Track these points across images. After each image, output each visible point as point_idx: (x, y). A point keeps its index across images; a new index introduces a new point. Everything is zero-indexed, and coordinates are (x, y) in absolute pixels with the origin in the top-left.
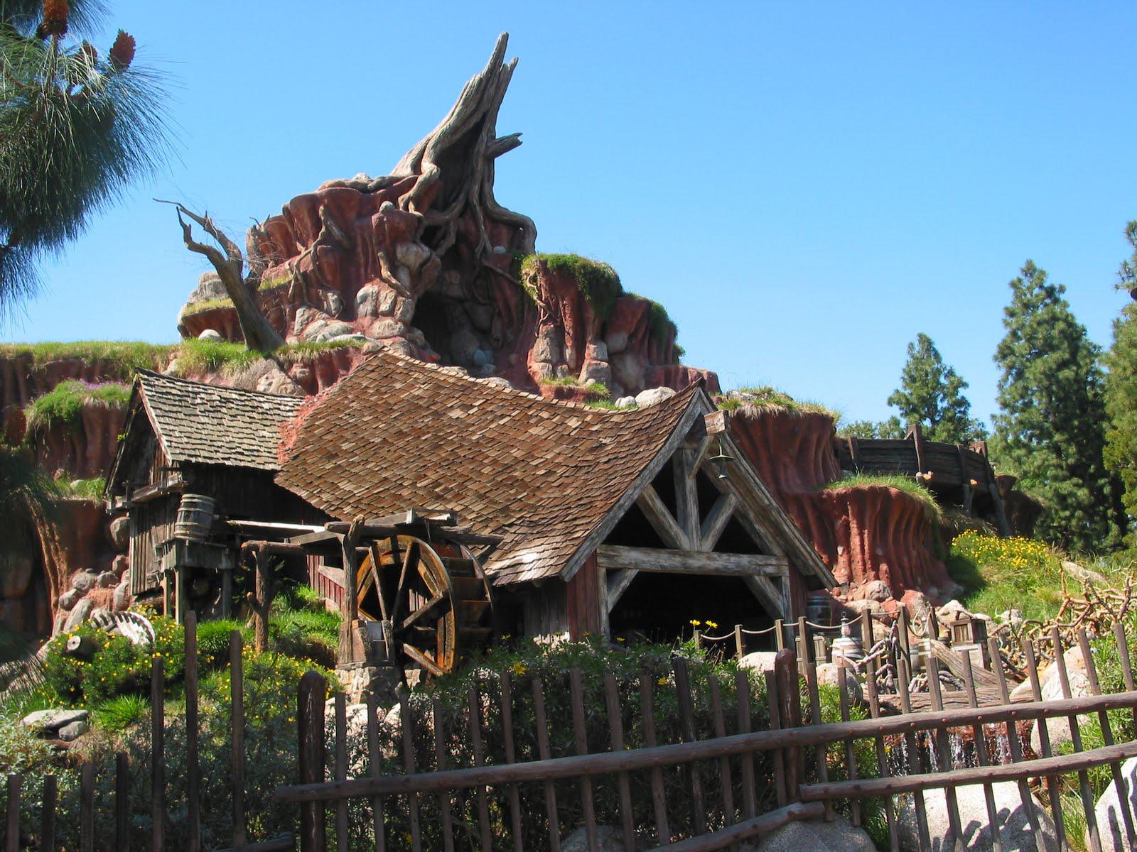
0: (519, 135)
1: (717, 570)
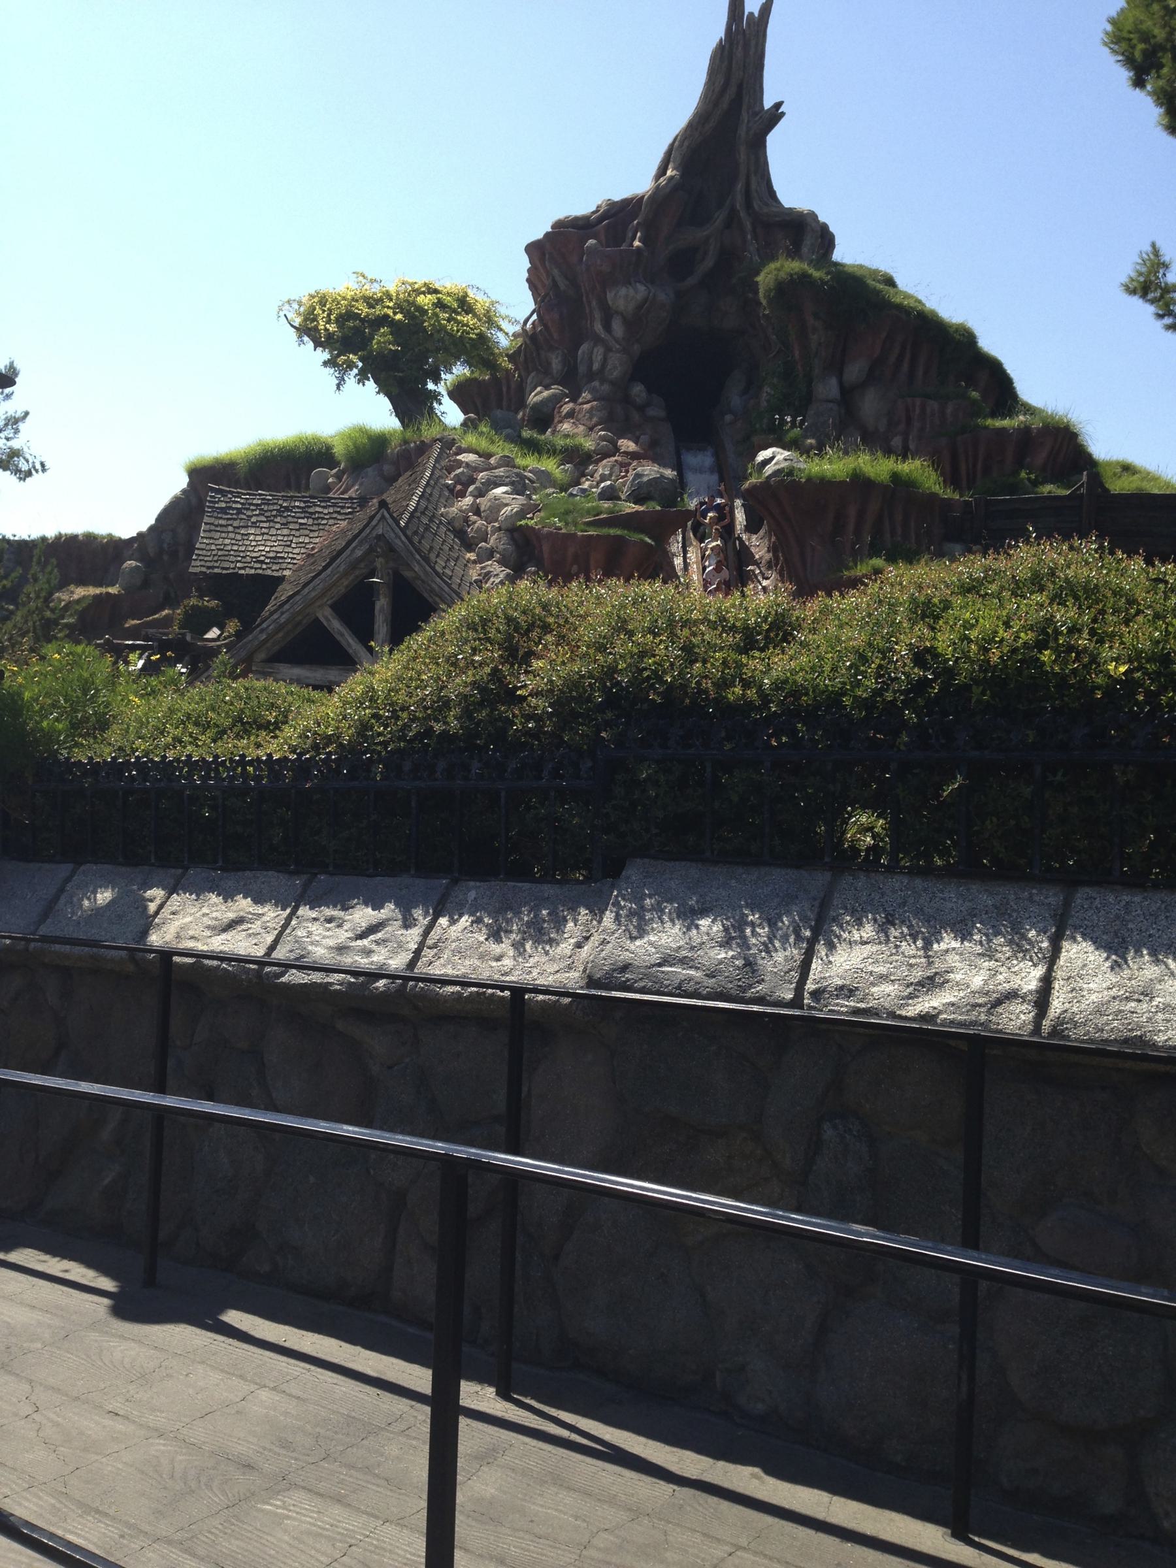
0: (778, 105)
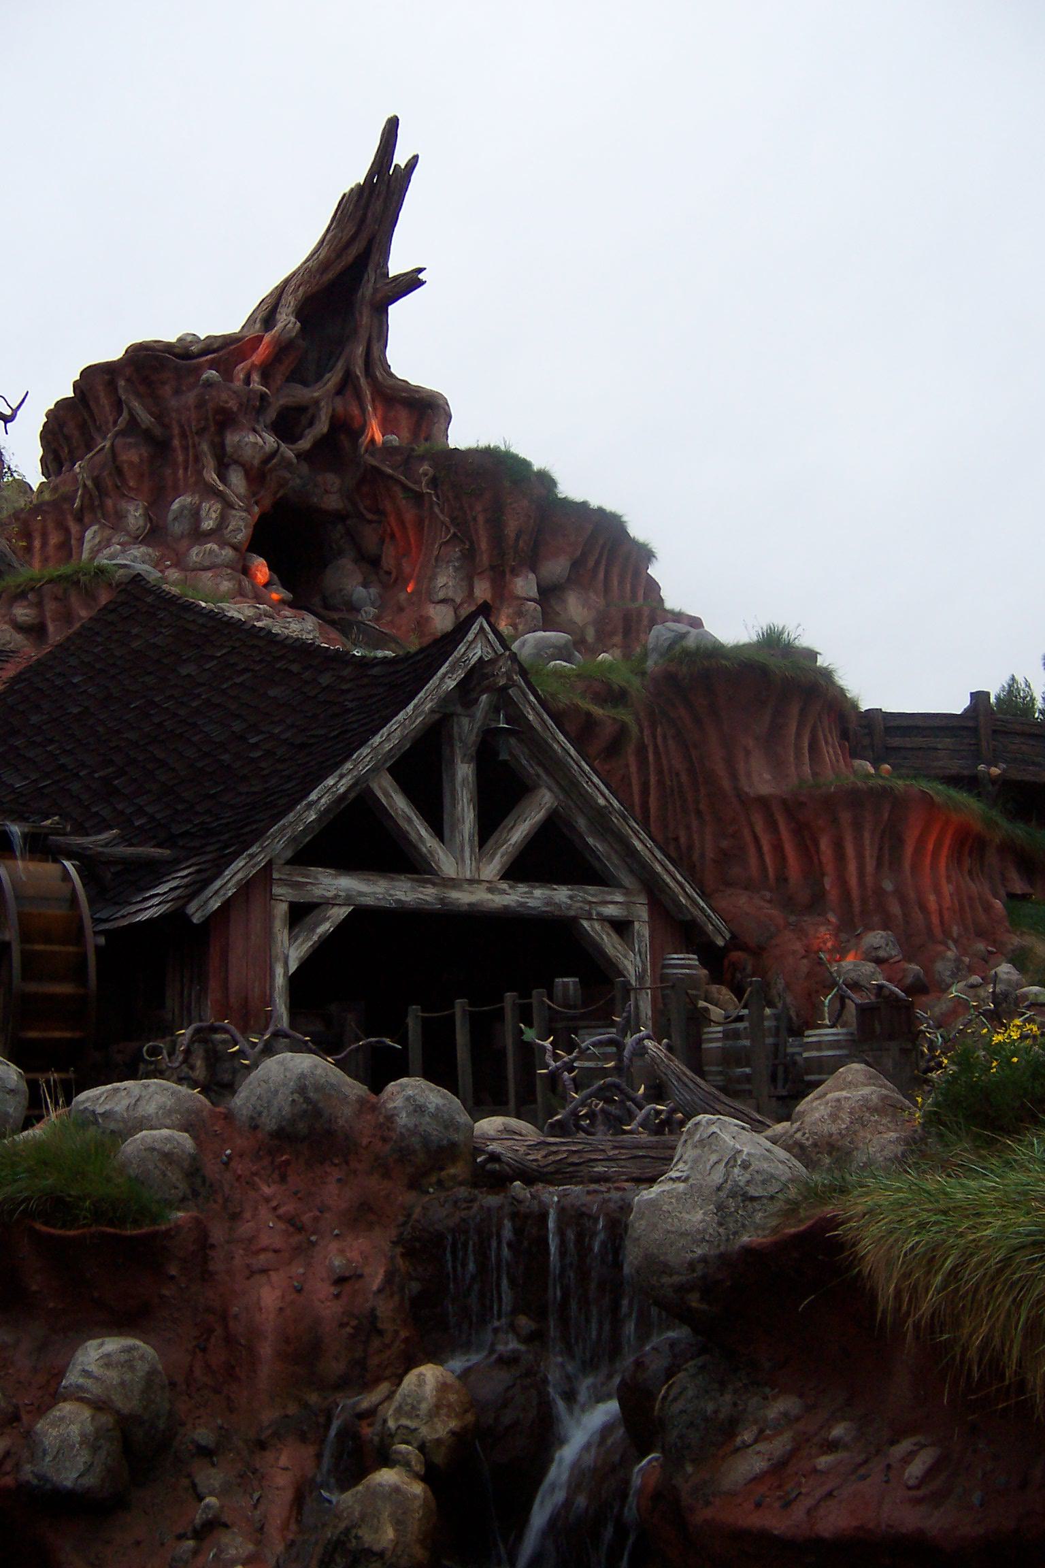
0: (420, 270)
1: (506, 907)
